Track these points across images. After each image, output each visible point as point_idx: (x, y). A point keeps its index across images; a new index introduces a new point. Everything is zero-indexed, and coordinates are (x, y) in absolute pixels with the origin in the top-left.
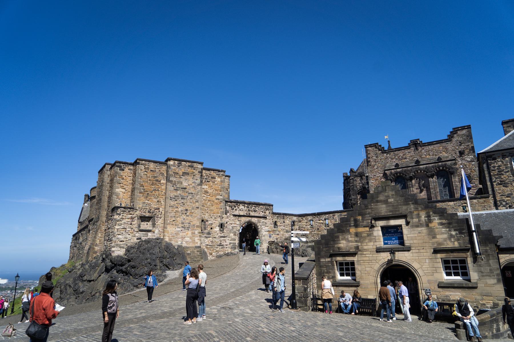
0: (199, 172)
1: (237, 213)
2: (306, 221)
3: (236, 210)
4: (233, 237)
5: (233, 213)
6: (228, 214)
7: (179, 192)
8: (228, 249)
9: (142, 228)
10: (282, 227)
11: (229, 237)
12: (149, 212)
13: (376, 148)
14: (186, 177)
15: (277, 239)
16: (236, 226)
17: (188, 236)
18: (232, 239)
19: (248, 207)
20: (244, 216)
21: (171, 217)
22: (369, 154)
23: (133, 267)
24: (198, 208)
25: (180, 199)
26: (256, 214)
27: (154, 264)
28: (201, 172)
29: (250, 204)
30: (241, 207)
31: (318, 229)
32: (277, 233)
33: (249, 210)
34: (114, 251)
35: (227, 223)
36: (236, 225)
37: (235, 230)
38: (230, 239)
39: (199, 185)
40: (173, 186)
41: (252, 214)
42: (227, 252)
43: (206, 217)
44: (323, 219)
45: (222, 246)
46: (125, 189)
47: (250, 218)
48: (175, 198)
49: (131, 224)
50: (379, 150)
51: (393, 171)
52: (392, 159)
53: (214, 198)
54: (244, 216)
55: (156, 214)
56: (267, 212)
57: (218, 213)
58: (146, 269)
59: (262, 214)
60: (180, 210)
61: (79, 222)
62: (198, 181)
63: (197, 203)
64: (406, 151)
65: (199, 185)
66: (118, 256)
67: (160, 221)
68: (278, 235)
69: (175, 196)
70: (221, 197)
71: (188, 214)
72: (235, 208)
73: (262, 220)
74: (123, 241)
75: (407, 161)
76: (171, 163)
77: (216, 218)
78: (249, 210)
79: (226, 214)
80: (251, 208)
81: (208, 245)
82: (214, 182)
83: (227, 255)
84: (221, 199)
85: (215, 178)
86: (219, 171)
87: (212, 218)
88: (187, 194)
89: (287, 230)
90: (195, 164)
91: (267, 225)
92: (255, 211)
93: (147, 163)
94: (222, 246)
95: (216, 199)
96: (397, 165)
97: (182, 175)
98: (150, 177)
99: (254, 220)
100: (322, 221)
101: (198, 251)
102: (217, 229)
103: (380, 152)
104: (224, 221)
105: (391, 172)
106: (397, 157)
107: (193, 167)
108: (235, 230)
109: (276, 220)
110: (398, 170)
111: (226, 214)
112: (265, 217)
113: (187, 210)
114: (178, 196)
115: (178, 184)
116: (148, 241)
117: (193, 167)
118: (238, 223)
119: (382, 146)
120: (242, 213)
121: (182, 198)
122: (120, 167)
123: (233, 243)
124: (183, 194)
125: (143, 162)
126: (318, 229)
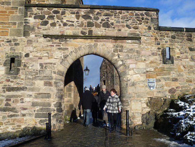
1: (56, 31)
3: (53, 25)
4: (44, 89)
5: (45, 33)
6: (32, 36)
11: (32, 90)
15: (172, 91)
19: (86, 17)
20: (75, 37)
26: (113, 32)
32: (173, 75)
33: (90, 25)
35: (27, 55)
37: (48, 72)
54: (75, 37)
56: (143, 27)
59: (126, 32)
68: (175, 80)
72: (50, 22)
73: (128, 44)
78: (90, 25)
79: (26, 34)
80: (97, 19)
104: (22, 50)
111: (26, 34)
112: (136, 38)
118: (59, 54)
120: (69, 31)
123: (43, 104)
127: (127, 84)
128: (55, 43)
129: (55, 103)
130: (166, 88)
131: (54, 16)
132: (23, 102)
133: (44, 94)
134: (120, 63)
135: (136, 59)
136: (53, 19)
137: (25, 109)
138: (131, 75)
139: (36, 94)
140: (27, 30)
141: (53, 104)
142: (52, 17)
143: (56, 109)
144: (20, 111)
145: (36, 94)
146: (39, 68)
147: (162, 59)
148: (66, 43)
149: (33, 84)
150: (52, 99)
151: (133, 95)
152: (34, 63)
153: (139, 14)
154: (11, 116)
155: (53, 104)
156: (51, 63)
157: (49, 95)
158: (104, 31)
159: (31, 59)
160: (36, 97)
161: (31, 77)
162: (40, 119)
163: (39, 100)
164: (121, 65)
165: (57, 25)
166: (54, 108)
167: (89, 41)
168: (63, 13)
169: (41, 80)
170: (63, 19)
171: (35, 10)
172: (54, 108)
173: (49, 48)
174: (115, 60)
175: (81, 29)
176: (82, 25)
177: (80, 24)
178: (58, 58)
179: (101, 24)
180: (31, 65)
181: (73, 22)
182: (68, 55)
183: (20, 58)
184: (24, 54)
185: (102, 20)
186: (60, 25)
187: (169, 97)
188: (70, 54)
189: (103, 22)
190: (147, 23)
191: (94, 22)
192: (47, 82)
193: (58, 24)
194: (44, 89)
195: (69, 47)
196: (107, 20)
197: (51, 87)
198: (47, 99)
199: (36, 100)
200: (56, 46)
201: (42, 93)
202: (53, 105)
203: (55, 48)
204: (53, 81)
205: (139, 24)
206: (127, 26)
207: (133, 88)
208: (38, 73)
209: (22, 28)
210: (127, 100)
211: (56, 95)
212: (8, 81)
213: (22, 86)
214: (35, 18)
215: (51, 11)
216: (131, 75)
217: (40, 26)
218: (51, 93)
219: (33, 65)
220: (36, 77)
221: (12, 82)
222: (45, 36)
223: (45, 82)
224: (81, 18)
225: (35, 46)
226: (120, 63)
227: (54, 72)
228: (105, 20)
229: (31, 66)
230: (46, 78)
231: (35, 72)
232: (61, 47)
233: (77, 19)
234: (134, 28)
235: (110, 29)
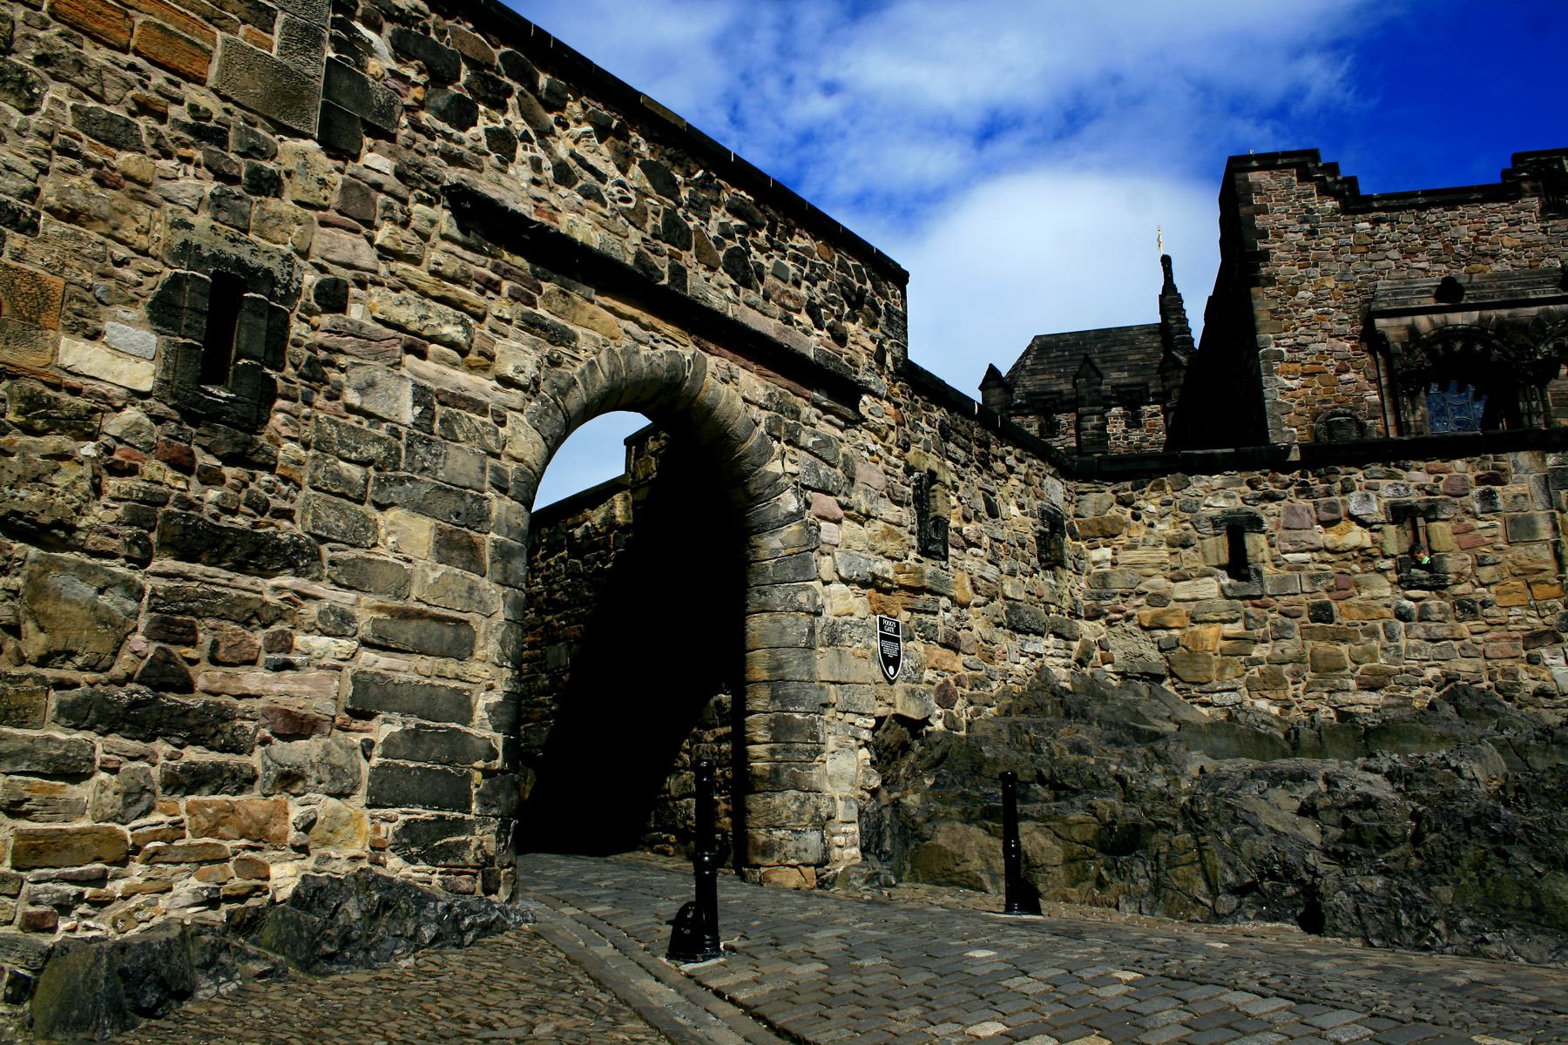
2: (1165, 528)
4: (431, 579)
6: (376, 161)
10: (973, 562)
11: (355, 578)
13: (1304, 177)
22: (1263, 210)
31: (1322, 613)
33: (674, 231)
35: (333, 297)
37: (460, 462)
38: (365, 609)
41: (713, 289)
44: (1375, 510)
50: (1325, 191)
51: (1423, 321)
52: (1411, 254)
64: (1497, 213)
75: (1504, 276)
89: (1013, 606)
91: (859, 499)
96: (1450, 294)
99: (738, 390)
100: (1357, 536)
103: (1330, 204)
105: (1413, 330)
106: (1438, 246)
108: (460, 462)
109: (932, 462)
110: (1458, 319)
112: (841, 391)
118: (518, 355)
119: (1345, 172)
126: (1322, 613)
127: (812, 631)
128: (507, 274)
129: (495, 698)
130: (929, 675)
131: (509, 91)
132: (289, 665)
133: (434, 625)
134: (790, 502)
135: (842, 498)
136: (503, 108)
137: (297, 726)
138: (826, 583)
139: (381, 616)
140: (347, 105)
141: (482, 702)
143: (498, 740)
144: (265, 741)
145: (380, 609)
146: (408, 413)
147: (916, 528)
148: (566, 295)
149: (360, 536)
150: (477, 669)
151: (833, 693)
152: (378, 371)
153: (850, 263)
155: (482, 702)
156: (482, 409)
157: (464, 632)
158: (729, 293)
159: (357, 333)
160: (380, 644)
161: (356, 472)
162: (400, 815)
163: (403, 668)
164: (793, 517)
165: (521, 153)
166: (488, 733)
169: (420, 509)
170: (552, 132)
172: (488, 733)
173: (470, 295)
174: (767, 480)
175: (635, 236)
176: (637, 218)
177: (631, 205)
178: (521, 379)
179: (721, 254)
180: (358, 376)
181: (602, 178)
182: (575, 382)
183: (283, 300)
184: (310, 279)
185: (726, 232)
186: (536, 165)
187: (939, 725)
188: (582, 373)
189: (729, 244)
190: (874, 325)
191: (691, 225)
192: (456, 537)
193: (529, 153)
194: (436, 582)
195: (579, 330)
196: (743, 242)
197: (476, 577)
198: (451, 667)
200: (515, 297)
201: (420, 615)
202: (486, 715)
203: (500, 306)
205: (848, 318)
206: (813, 310)
207: (829, 652)
208: (403, 453)
209: (316, 71)
210: (812, 723)
211: (502, 643)
213: (286, 531)
215: (497, 53)
216: (826, 583)
217: (425, 117)
218: (475, 618)
219: (372, 384)
220: (387, 479)
221: (211, 478)
223: (441, 531)
224: (635, 170)
225: (389, 244)
226: (790, 502)
227: (495, 469)
228: (732, 237)
229: (361, 390)
230: (451, 503)
231: (379, 440)
232: (541, 311)
233: (619, 167)
234: (830, 329)
235: (753, 296)
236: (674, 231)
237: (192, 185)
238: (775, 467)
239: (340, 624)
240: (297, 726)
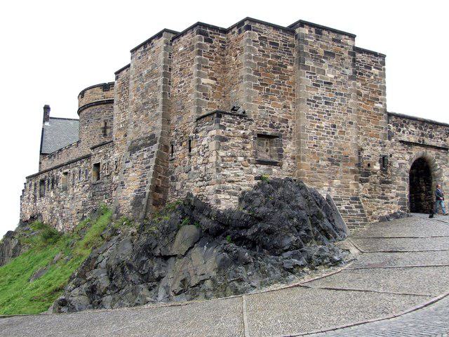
0: (349, 53)
1: (405, 138)
3: (404, 132)
6: (393, 140)
7: (320, 90)
8: (394, 205)
9: (259, 158)
12: (271, 126)
14: (334, 61)
16: (403, 161)
17: (338, 175)
18: (400, 188)
19: (421, 129)
20: (416, 144)
21: (311, 138)
23: (269, 232)
24: (351, 123)
25: (323, 104)
26: (434, 144)
27: (305, 227)
28: (354, 55)
29: (424, 122)
30: (412, 128)
34: (218, 202)
35: (391, 156)
36: (403, 161)
37: (403, 170)
39: (351, 78)
40: (311, 77)
41: (428, 141)
42: (393, 211)
43: (361, 143)
45: (386, 198)
46: (216, 79)
47: (424, 150)
48: (314, 102)
49: (243, 149)
53: (370, 108)
54: (416, 144)
55: (282, 131)
57: (377, 136)
58: (293, 238)
59: (440, 143)
60: (323, 124)
61: (41, 154)
62: (349, 72)
63: (349, 114)
65: (351, 78)
66: (230, 211)
67: (289, 146)
69: (315, 98)
70: (381, 106)
71: (336, 134)
73: (441, 153)
74: (233, 182)
76: (305, 30)
77: (374, 146)
78: (423, 135)
80: (425, 130)
81: (364, 196)
82: (369, 76)
83: (395, 216)
84: (381, 109)
85: (370, 68)
86: (375, 54)
87: (368, 144)
88: (334, 95)
90: (343, 37)
92: (431, 137)
93: (263, 27)
94: (386, 198)
95: (374, 109)
97: (324, 58)
98: (269, 57)
99: (431, 154)
101: (357, 207)
102: (377, 167)
104: (389, 151)
107: (339, 41)
111: (390, 139)
113: (334, 126)
114: (320, 98)
115: (318, 72)
116: (276, 184)
117: (339, 41)
118: (407, 157)
120: (412, 140)
121: (326, 103)
122: (205, 34)
124: (327, 95)
125: (257, 25)
137: (392, 198)
142: (402, 126)
154: (386, 203)
167: (423, 148)
168: (408, 124)
171: (394, 119)
199: (397, 192)
203: (405, 152)
204: (406, 178)
206: (441, 138)
212: (382, 175)
214: (394, 125)
222: (401, 142)
236: (423, 135)
237: (380, 148)
238: (436, 163)
239: (394, 188)
240: (392, 198)
